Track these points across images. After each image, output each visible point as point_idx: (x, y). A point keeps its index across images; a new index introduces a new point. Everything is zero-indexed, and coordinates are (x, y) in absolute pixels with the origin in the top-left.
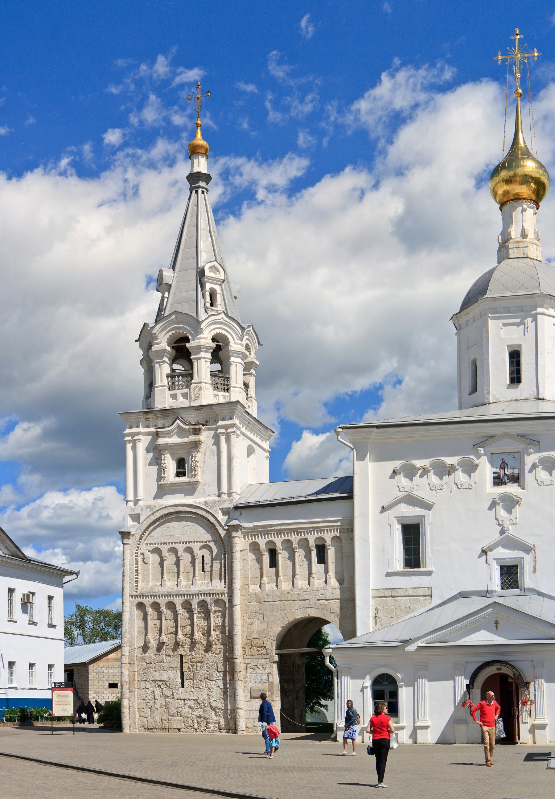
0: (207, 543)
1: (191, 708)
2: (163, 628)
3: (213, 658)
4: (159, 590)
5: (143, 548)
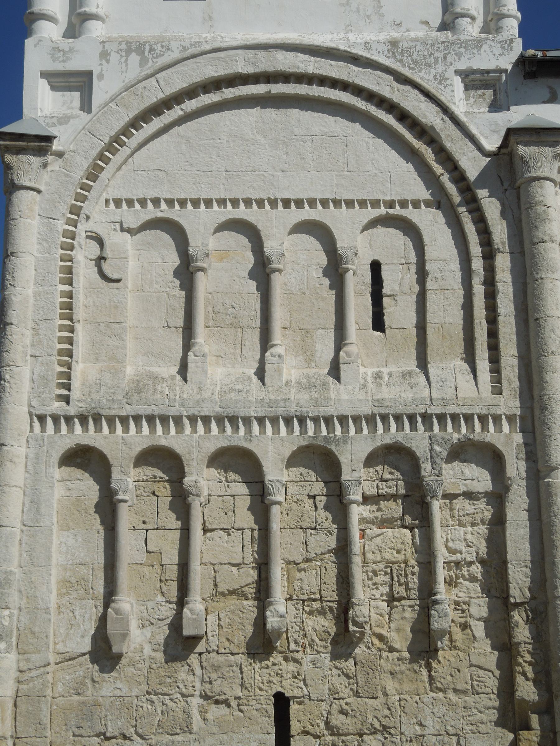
0: (397, 210)
2: (196, 567)
3: (441, 710)
4: (181, 397)
5: (99, 217)
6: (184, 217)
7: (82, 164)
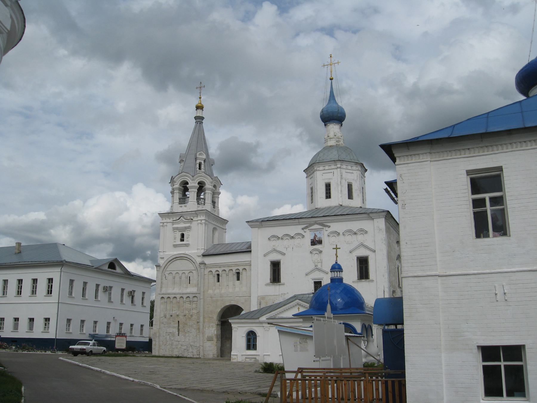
7: (163, 267)
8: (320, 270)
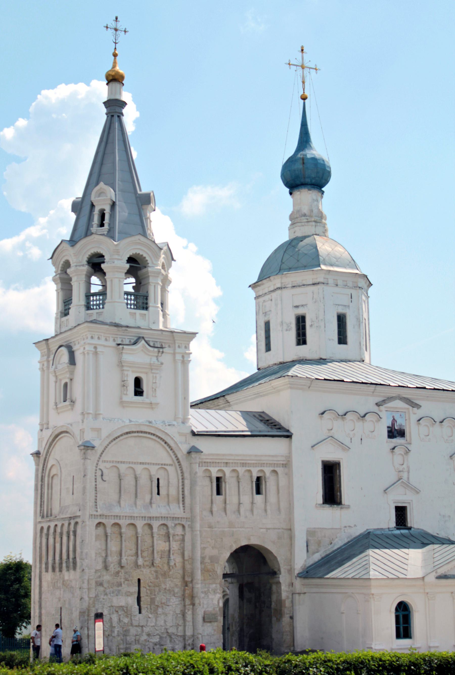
0: (163, 466)
1: (149, 635)
6: (118, 465)
7: (99, 452)
8: (407, 485)
